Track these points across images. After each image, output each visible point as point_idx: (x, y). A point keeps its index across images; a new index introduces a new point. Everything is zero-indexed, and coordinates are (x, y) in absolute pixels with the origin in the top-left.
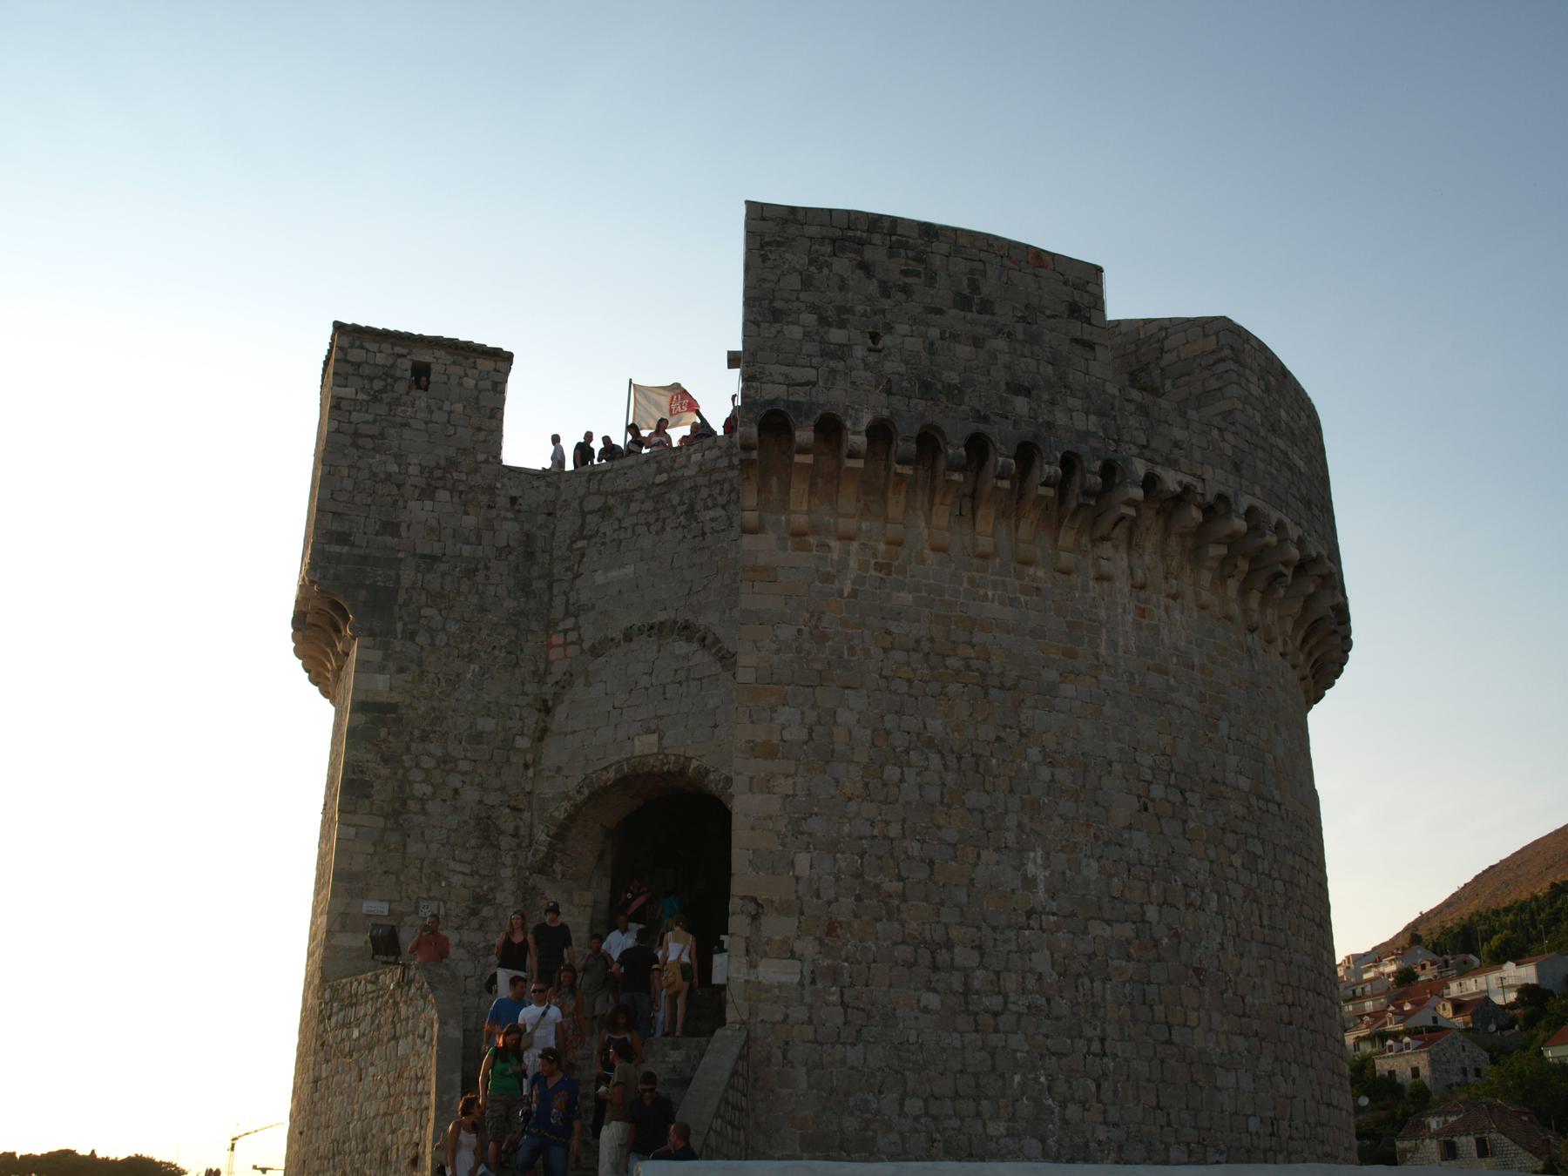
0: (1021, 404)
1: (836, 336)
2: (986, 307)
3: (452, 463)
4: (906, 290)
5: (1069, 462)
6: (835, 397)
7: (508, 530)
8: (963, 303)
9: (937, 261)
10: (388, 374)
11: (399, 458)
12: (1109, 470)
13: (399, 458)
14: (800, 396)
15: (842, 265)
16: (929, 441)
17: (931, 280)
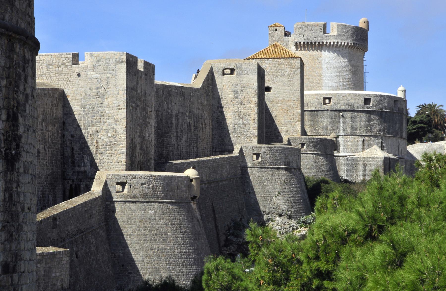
0: (315, 38)
1: (301, 35)
2: (312, 31)
3: (280, 38)
4: (306, 31)
5: (319, 43)
6: (300, 41)
7: (285, 44)
8: (311, 31)
9: (308, 27)
10: (273, 30)
11: (275, 38)
12: (323, 42)
13: (275, 38)
14: (298, 41)
15: (301, 29)
16: (308, 43)
17: (308, 29)
